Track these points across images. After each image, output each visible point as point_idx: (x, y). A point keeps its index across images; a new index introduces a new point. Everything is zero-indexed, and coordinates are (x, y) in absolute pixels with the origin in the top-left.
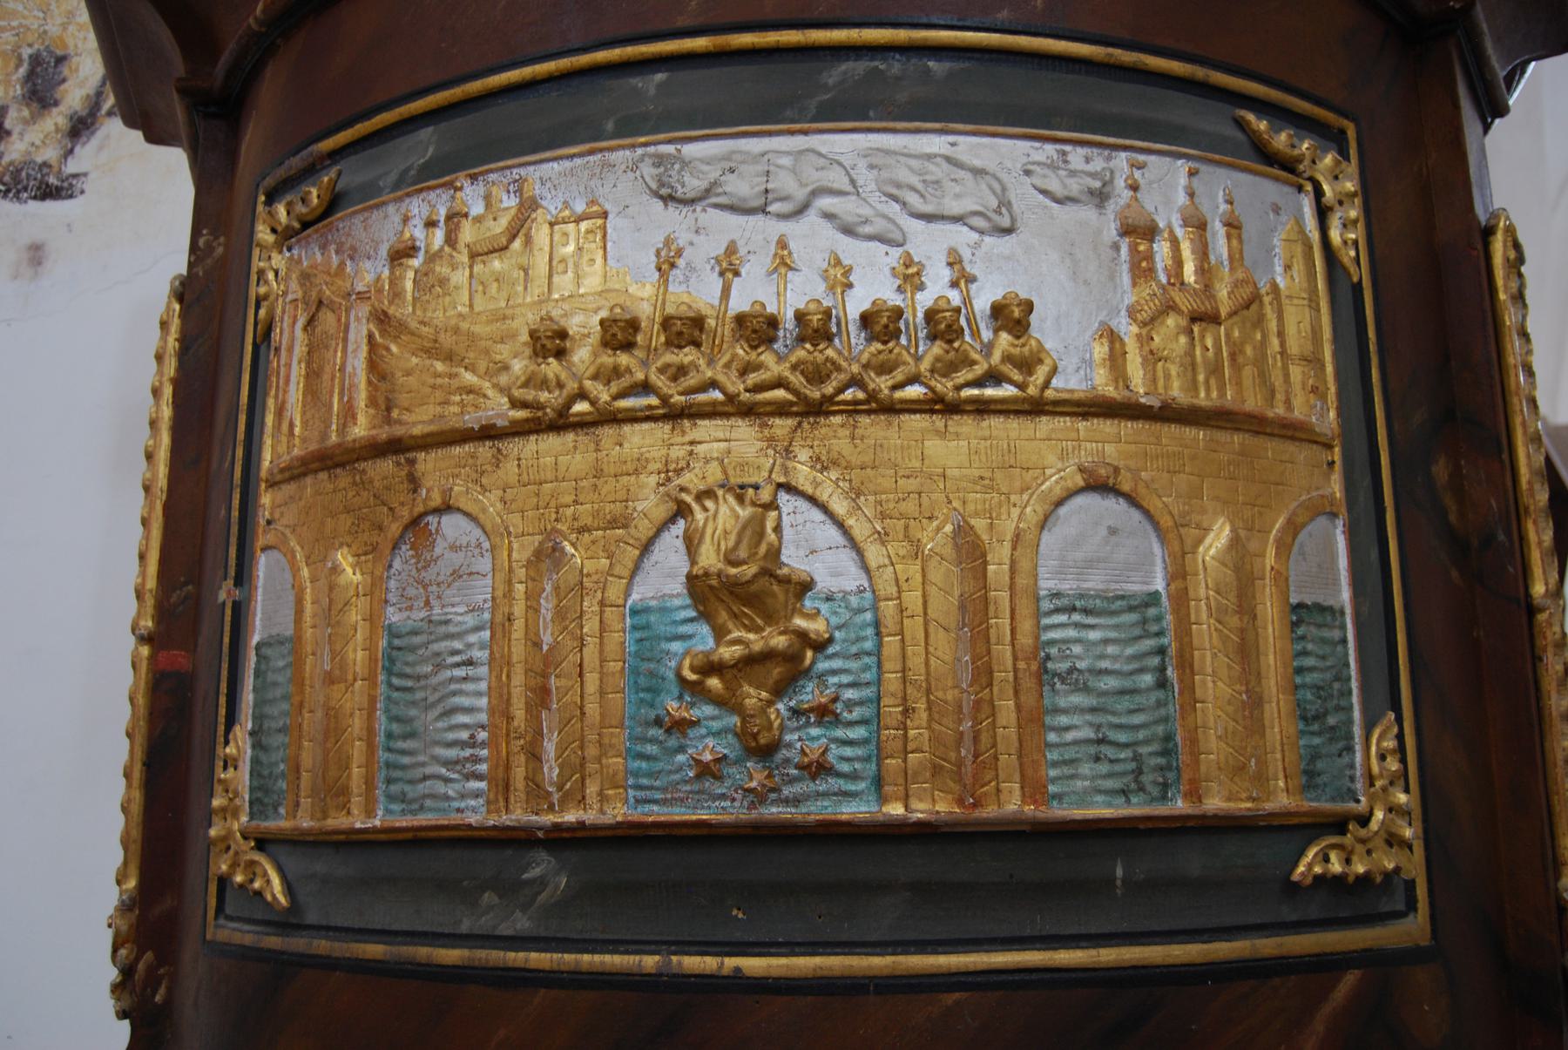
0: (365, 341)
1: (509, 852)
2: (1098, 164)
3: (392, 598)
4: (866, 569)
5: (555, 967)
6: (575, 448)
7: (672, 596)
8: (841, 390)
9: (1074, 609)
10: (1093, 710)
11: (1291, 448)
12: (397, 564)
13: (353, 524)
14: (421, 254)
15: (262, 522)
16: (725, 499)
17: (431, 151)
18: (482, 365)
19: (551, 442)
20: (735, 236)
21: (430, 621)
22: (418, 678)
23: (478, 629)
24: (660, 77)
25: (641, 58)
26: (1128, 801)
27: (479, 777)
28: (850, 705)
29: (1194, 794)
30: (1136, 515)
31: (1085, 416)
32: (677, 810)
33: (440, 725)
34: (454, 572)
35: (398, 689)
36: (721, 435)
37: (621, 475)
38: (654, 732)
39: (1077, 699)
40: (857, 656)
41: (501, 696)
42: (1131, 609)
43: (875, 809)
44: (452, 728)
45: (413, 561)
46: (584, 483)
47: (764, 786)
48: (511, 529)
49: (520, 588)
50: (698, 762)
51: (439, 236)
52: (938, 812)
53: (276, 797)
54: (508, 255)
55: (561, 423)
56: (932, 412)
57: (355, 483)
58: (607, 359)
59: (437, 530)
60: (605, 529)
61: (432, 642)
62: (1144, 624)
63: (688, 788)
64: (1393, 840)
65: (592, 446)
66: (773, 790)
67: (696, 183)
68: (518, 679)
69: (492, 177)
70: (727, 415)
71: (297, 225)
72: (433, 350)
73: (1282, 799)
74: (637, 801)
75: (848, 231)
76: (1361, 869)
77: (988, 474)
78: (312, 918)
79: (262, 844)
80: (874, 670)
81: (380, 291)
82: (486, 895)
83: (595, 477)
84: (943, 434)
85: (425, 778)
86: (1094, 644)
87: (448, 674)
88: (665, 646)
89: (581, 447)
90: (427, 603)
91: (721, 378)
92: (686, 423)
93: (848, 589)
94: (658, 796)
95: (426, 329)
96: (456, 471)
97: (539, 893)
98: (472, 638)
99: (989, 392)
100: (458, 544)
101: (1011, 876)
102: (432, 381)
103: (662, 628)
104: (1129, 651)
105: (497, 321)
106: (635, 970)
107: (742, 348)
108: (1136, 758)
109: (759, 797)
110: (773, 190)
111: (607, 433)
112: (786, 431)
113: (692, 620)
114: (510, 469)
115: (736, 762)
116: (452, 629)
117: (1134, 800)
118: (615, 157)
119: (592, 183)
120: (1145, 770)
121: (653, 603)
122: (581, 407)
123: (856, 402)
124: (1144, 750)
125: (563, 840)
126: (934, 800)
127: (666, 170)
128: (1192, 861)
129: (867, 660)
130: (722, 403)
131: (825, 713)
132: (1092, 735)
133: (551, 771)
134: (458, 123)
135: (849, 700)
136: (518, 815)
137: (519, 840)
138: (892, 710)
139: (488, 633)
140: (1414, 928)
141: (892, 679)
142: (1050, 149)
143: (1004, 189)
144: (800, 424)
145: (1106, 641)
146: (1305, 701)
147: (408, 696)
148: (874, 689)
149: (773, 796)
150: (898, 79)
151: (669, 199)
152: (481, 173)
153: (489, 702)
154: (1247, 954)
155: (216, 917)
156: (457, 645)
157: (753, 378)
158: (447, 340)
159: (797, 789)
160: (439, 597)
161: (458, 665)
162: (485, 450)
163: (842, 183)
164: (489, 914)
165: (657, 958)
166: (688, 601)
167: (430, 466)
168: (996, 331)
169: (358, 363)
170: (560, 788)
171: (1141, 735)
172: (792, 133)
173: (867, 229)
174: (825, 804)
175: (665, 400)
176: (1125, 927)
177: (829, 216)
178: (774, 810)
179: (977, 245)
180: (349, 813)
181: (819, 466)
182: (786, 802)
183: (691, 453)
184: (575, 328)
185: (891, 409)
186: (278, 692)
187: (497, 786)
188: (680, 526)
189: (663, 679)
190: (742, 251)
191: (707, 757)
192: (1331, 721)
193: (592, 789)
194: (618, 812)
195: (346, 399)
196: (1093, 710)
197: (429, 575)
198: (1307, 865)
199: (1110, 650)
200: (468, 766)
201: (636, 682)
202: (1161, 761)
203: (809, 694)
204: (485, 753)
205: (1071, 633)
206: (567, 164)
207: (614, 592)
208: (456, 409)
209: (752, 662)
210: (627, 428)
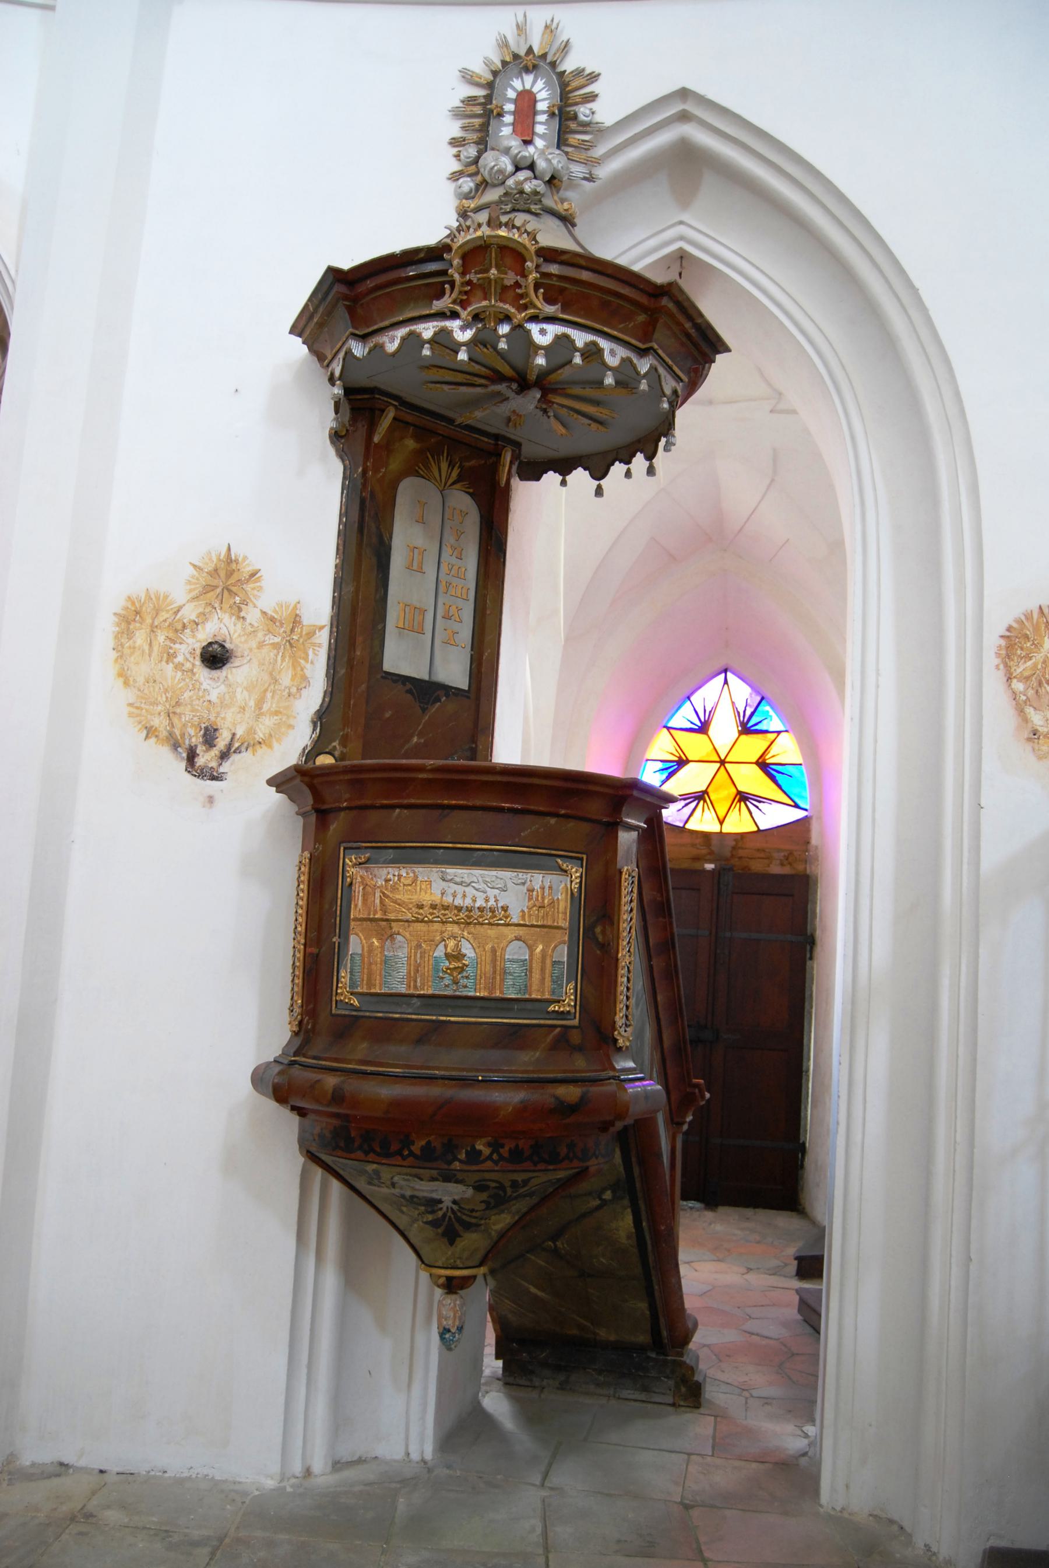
2: (525, 877)
11: (557, 931)
19: (420, 924)
24: (442, 851)
29: (530, 995)
30: (524, 945)
39: (511, 977)
51: (396, 878)
55: (422, 921)
58: (431, 911)
64: (569, 1005)
68: (412, 968)
72: (395, 902)
73: (547, 996)
76: (562, 1009)
78: (363, 1009)
79: (352, 994)
84: (491, 929)
99: (499, 922)
109: (455, 991)
111: (430, 924)
118: (433, 869)
125: (419, 996)
128: (529, 1006)
131: (467, 977)
133: (419, 984)
136: (411, 991)
137: (412, 996)
138: (478, 977)
140: (576, 1022)
141: (479, 972)
142: (516, 873)
151: (444, 880)
157: (458, 917)
158: (399, 901)
162: (406, 924)
163: (476, 881)
169: (378, 901)
175: (442, 920)
177: (473, 887)
185: (482, 924)
188: (443, 943)
193: (425, 988)
194: (430, 992)
197: (394, 946)
198: (551, 1008)
203: (465, 974)
207: (431, 954)
209: (455, 968)
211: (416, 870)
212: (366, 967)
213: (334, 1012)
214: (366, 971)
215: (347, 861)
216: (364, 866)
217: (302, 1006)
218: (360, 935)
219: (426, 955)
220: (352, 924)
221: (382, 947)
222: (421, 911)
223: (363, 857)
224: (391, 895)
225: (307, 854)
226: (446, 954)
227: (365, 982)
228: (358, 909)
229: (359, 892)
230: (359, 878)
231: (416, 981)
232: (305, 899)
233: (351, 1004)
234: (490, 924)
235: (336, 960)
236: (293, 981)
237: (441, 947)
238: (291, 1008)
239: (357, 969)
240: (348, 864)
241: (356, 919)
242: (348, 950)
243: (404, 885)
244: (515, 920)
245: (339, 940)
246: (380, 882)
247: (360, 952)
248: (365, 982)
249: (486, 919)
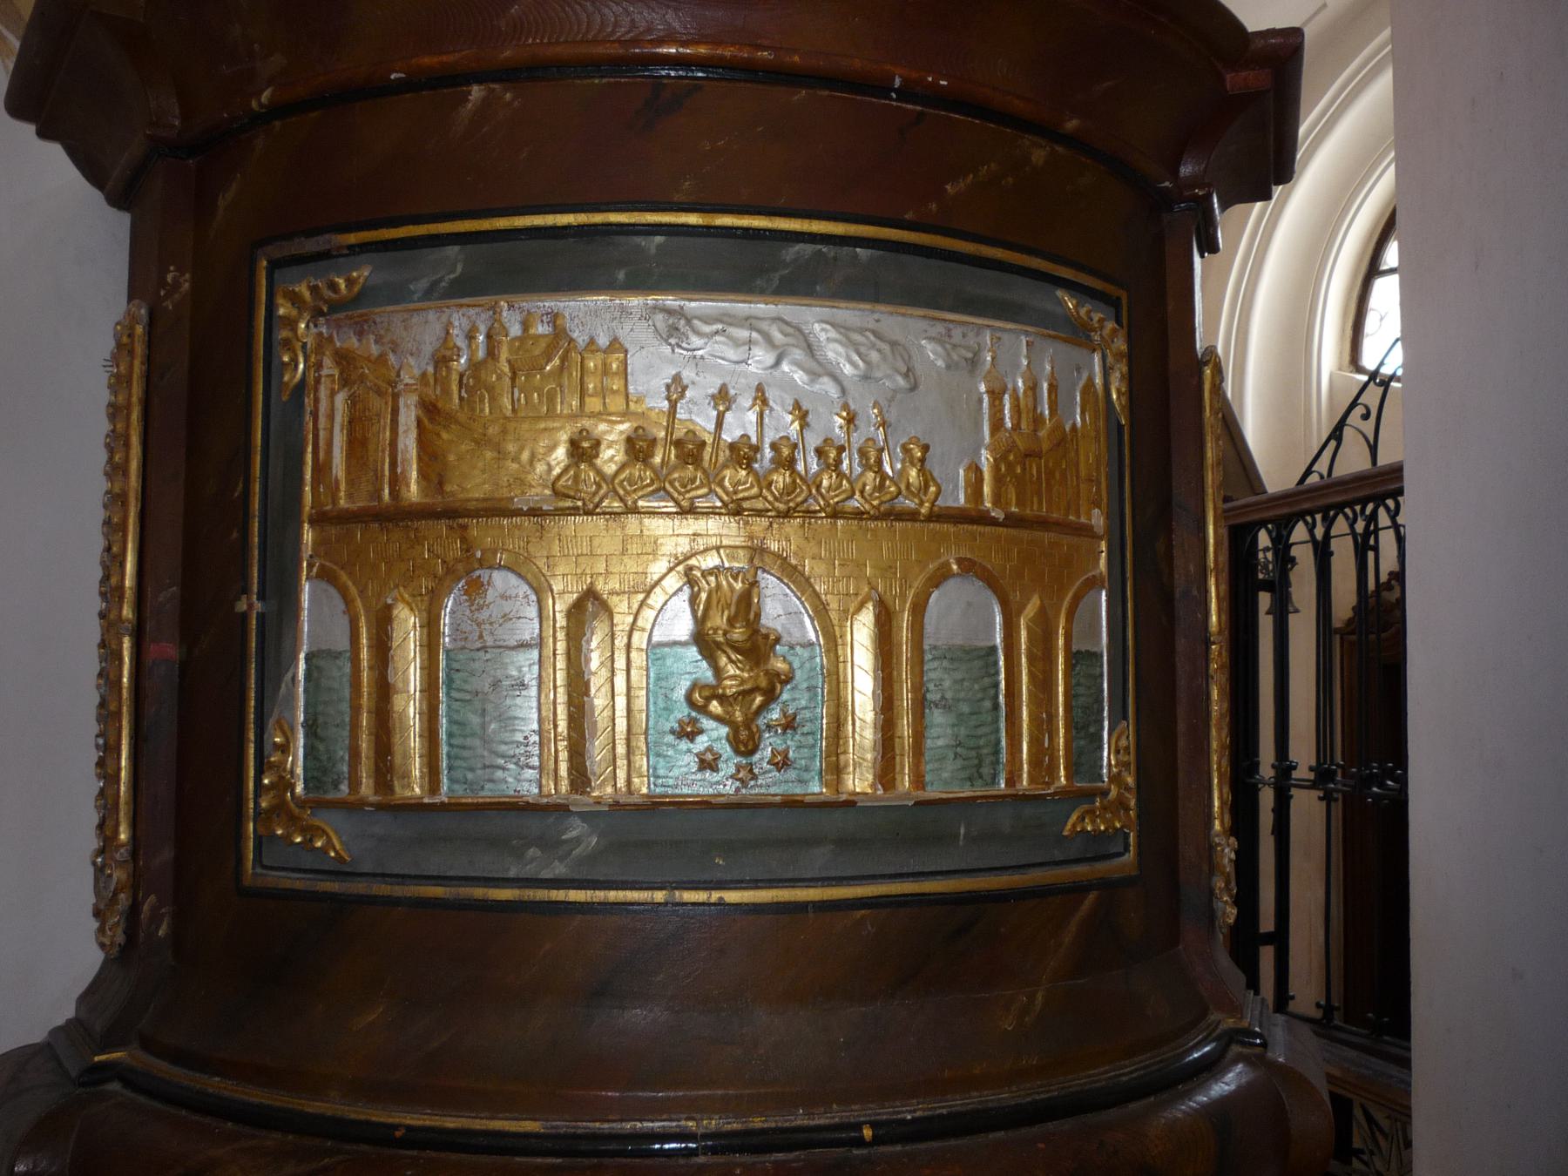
0: (415, 424)
2: (972, 341)
17: (459, 268)
20: (727, 380)
24: (659, 239)
45: (467, 604)
53: (336, 777)
59: (489, 584)
63: (694, 777)
70: (720, 514)
90: (481, 637)
97: (575, 849)
100: (508, 594)
108: (979, 757)
143: (910, 357)
149: (752, 783)
150: (835, 259)
160: (492, 633)
165: (664, 892)
185: (835, 514)
190: (732, 392)
192: (1092, 730)
197: (484, 615)
202: (993, 758)
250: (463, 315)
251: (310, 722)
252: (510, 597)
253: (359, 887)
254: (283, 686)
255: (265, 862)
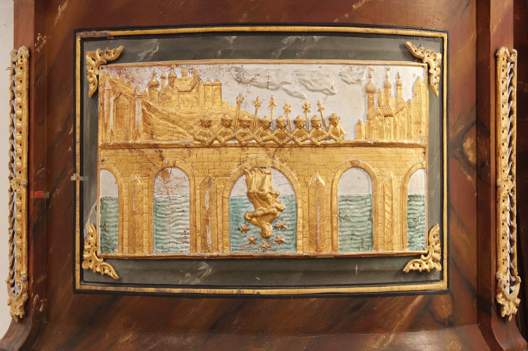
1: (195, 262)
3: (155, 191)
4: (294, 190)
5: (209, 293)
6: (214, 153)
7: (242, 196)
8: (288, 142)
9: (347, 200)
10: (351, 227)
12: (157, 181)
13: (140, 167)
14: (160, 86)
15: (100, 160)
16: (257, 172)
18: (185, 126)
19: (206, 150)
21: (170, 199)
22: (167, 215)
23: (185, 202)
24: (234, 37)
25: (228, 31)
26: (359, 250)
27: (187, 243)
28: (289, 226)
29: (377, 249)
31: (353, 147)
32: (244, 252)
33: (174, 228)
34: (177, 185)
35: (159, 217)
36: (255, 152)
37: (227, 162)
38: (238, 232)
39: (347, 224)
40: (291, 213)
41: (194, 221)
42: (363, 199)
43: (295, 252)
44: (178, 229)
45: (162, 181)
46: (217, 163)
47: (267, 246)
48: (195, 174)
49: (198, 191)
50: (250, 240)
51: (167, 82)
52: (311, 253)
53: (113, 246)
54: (191, 93)
55: (210, 146)
56: (312, 147)
57: (140, 155)
58: (223, 129)
60: (223, 177)
61: (171, 205)
62: (366, 203)
65: (219, 153)
66: (269, 247)
67: (248, 78)
68: (198, 216)
69: (183, 66)
70: (257, 147)
71: (105, 61)
72: (167, 118)
74: (233, 249)
75: (290, 94)
77: (326, 164)
78: (125, 281)
79: (105, 259)
80: (295, 216)
81: (146, 96)
82: (187, 274)
83: (220, 162)
84: (314, 153)
85: (170, 242)
86: (352, 209)
87: (177, 214)
88: (241, 209)
89: (215, 153)
90: (168, 193)
91: (256, 137)
92: (246, 148)
93: (289, 195)
94: (239, 248)
95: (165, 112)
96: (176, 156)
98: (183, 205)
100: (178, 177)
101: (328, 269)
102: (167, 128)
103: (240, 205)
104: (361, 211)
105: (189, 114)
106: (231, 293)
107: (262, 129)
108: (362, 239)
109: (265, 249)
110: (270, 82)
111: (223, 149)
112: (273, 152)
113: (248, 203)
114: (194, 157)
115: (260, 240)
116: (177, 201)
117: (361, 250)
119: (216, 74)
120: (364, 242)
121: (237, 198)
122: (216, 142)
123: (292, 145)
124: (364, 237)
125: (210, 260)
126: (310, 250)
127: (239, 73)
128: (377, 266)
129: (293, 214)
130: (256, 144)
132: (351, 233)
133: (209, 241)
134: (166, 40)
135: (289, 224)
136: (199, 253)
137: (199, 259)
139: (189, 203)
140: (442, 285)
142: (347, 67)
144: (277, 150)
145: (356, 208)
146: (410, 222)
147: (163, 219)
148: (295, 221)
150: (304, 41)
151: (240, 82)
152: (180, 64)
153: (190, 222)
154: (390, 290)
155: (80, 282)
156: (179, 206)
158: (173, 117)
159: (275, 247)
160: (172, 192)
161: (180, 212)
162: (186, 151)
164: (188, 278)
165: (237, 290)
166: (247, 198)
167: (167, 153)
168: (330, 124)
169: (139, 118)
170: (212, 246)
171: (363, 233)
172: (275, 63)
173: (296, 94)
174: (282, 251)
175: (240, 143)
176: (358, 282)
177: (285, 90)
178: (269, 252)
179: (326, 98)
180: (143, 251)
181: (281, 162)
182: (272, 250)
183: (247, 157)
184: (213, 119)
186: (112, 215)
187: (193, 245)
189: (240, 218)
191: (252, 239)
193: (220, 246)
194: (227, 252)
195: (136, 129)
196: (351, 227)
197: (168, 185)
199: (356, 211)
200: (183, 239)
201: (232, 219)
204: (189, 236)
205: (346, 206)
206: (208, 66)
207: (226, 194)
208: (176, 138)
210: (229, 149)
211: (197, 68)
212: (126, 218)
213: (78, 287)
214: (126, 224)
215: (88, 58)
216: (113, 65)
217: (28, 279)
218: (115, 170)
219: (219, 197)
220: (102, 154)
221: (151, 188)
222: (208, 131)
223: (112, 51)
224: (160, 108)
225: (24, 51)
226: (249, 194)
227: (125, 241)
228: (109, 131)
229: (109, 106)
230: (107, 84)
231: (204, 237)
232: (25, 118)
233: (106, 275)
234: (313, 145)
235: (78, 209)
236: (12, 240)
237: (241, 183)
238: (12, 282)
239: (112, 221)
240: (89, 64)
241: (106, 147)
242: (97, 194)
243: (180, 92)
244: (350, 137)
245: (81, 178)
246: (144, 89)
247: (116, 196)
248: (125, 241)
249: (307, 139)
250: (159, 69)
251: (103, 225)
252: (179, 178)
253: (123, 289)
254: (91, 210)
255: (85, 280)
